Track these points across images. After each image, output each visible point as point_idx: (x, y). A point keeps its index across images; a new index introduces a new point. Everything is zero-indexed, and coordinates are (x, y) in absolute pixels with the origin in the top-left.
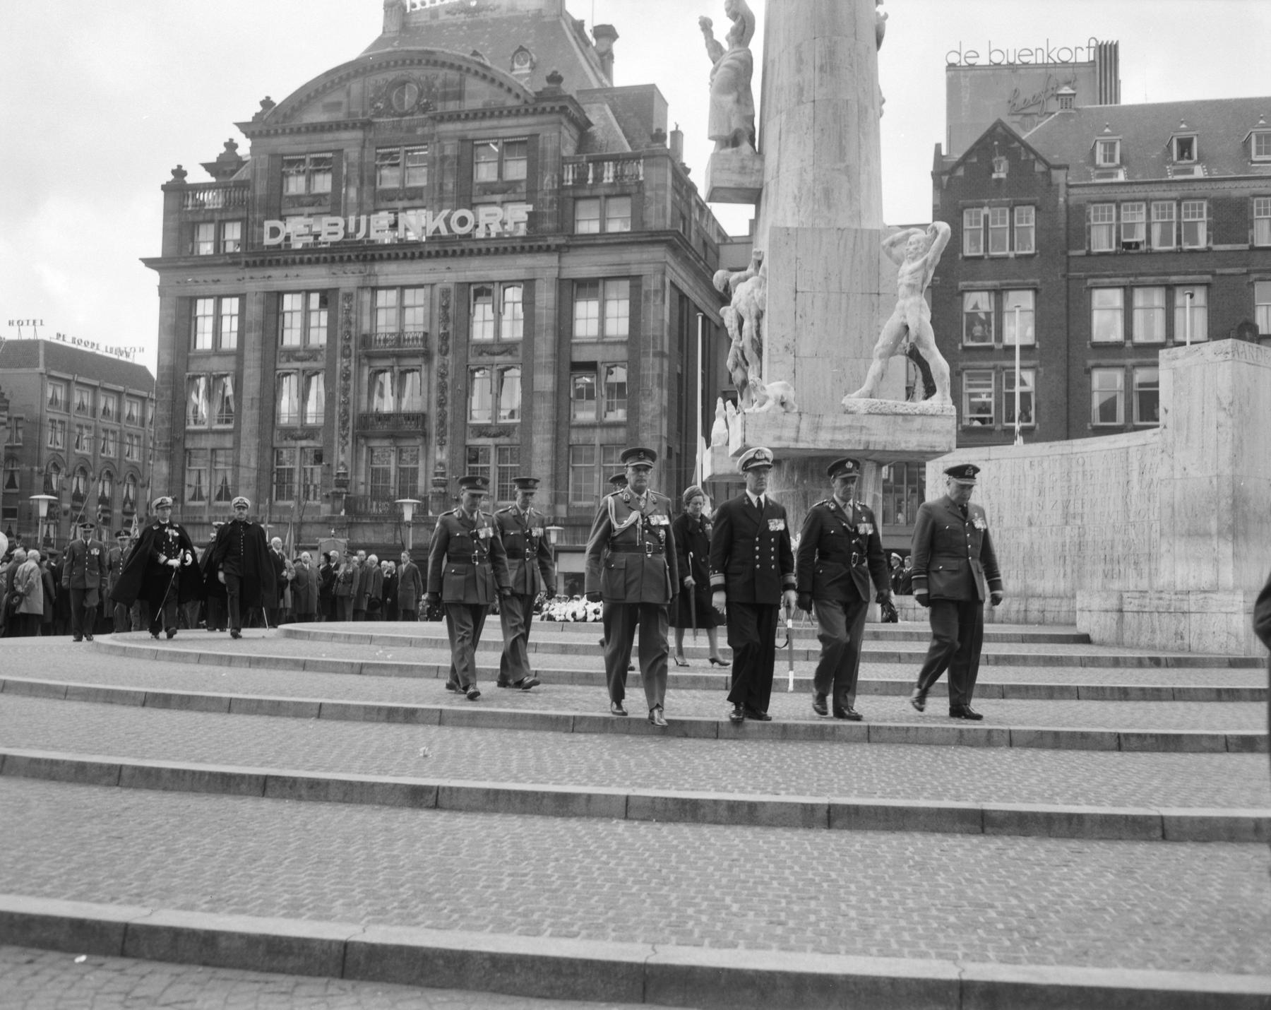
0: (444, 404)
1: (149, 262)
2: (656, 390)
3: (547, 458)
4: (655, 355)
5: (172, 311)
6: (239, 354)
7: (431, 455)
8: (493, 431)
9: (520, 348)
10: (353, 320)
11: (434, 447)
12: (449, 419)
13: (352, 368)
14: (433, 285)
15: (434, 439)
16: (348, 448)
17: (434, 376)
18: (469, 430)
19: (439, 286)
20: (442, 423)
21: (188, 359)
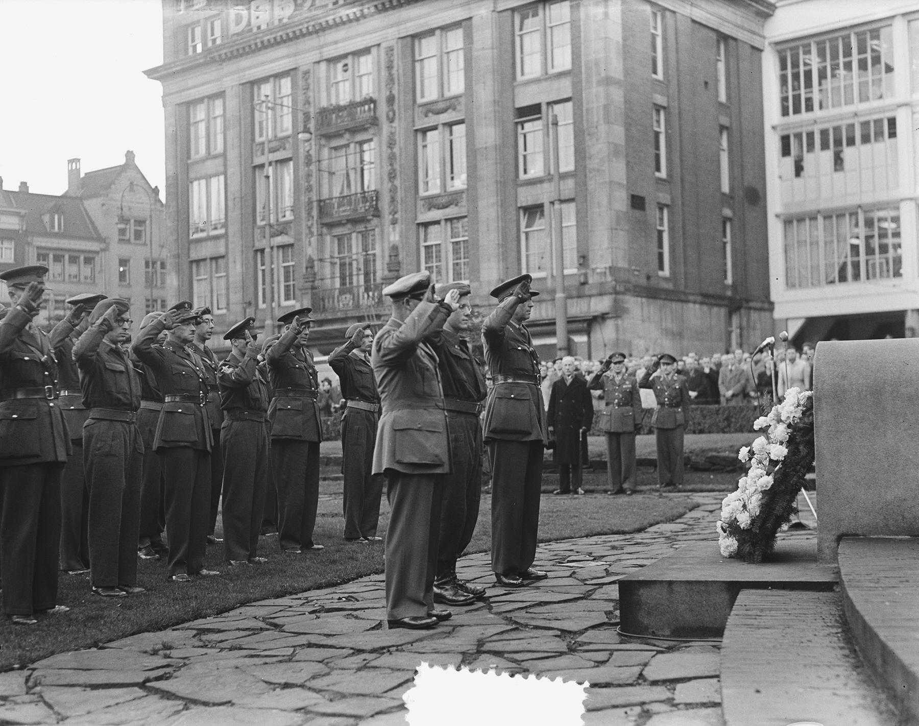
0: (394, 177)
1: (151, 73)
2: (603, 128)
3: (493, 226)
4: (599, 83)
5: (172, 121)
6: (224, 155)
7: (386, 237)
8: (444, 200)
9: (463, 100)
10: (311, 100)
11: (389, 228)
12: (399, 195)
13: (312, 152)
14: (379, 45)
15: (387, 218)
16: (314, 240)
17: (384, 148)
18: (420, 203)
19: (383, 45)
20: (393, 199)
21: (188, 165)
